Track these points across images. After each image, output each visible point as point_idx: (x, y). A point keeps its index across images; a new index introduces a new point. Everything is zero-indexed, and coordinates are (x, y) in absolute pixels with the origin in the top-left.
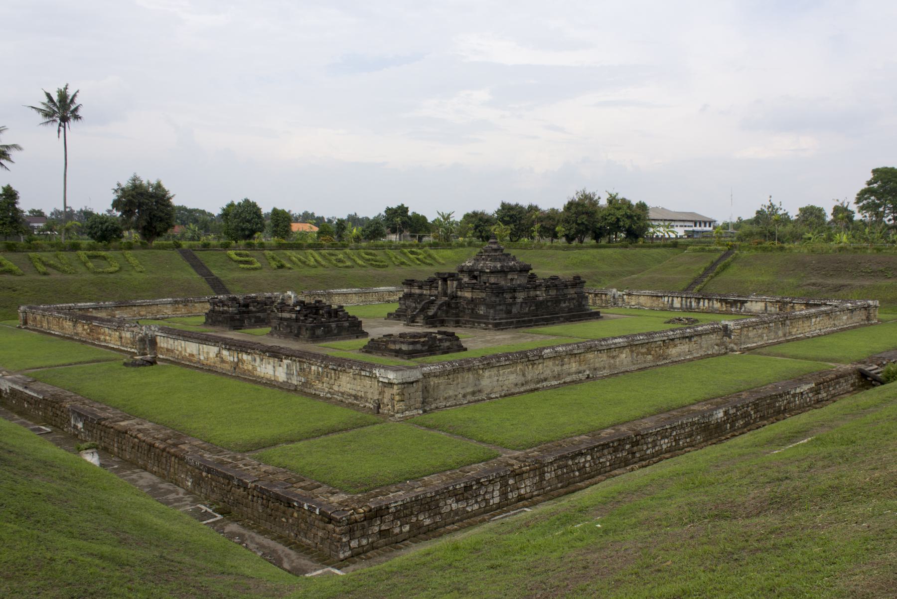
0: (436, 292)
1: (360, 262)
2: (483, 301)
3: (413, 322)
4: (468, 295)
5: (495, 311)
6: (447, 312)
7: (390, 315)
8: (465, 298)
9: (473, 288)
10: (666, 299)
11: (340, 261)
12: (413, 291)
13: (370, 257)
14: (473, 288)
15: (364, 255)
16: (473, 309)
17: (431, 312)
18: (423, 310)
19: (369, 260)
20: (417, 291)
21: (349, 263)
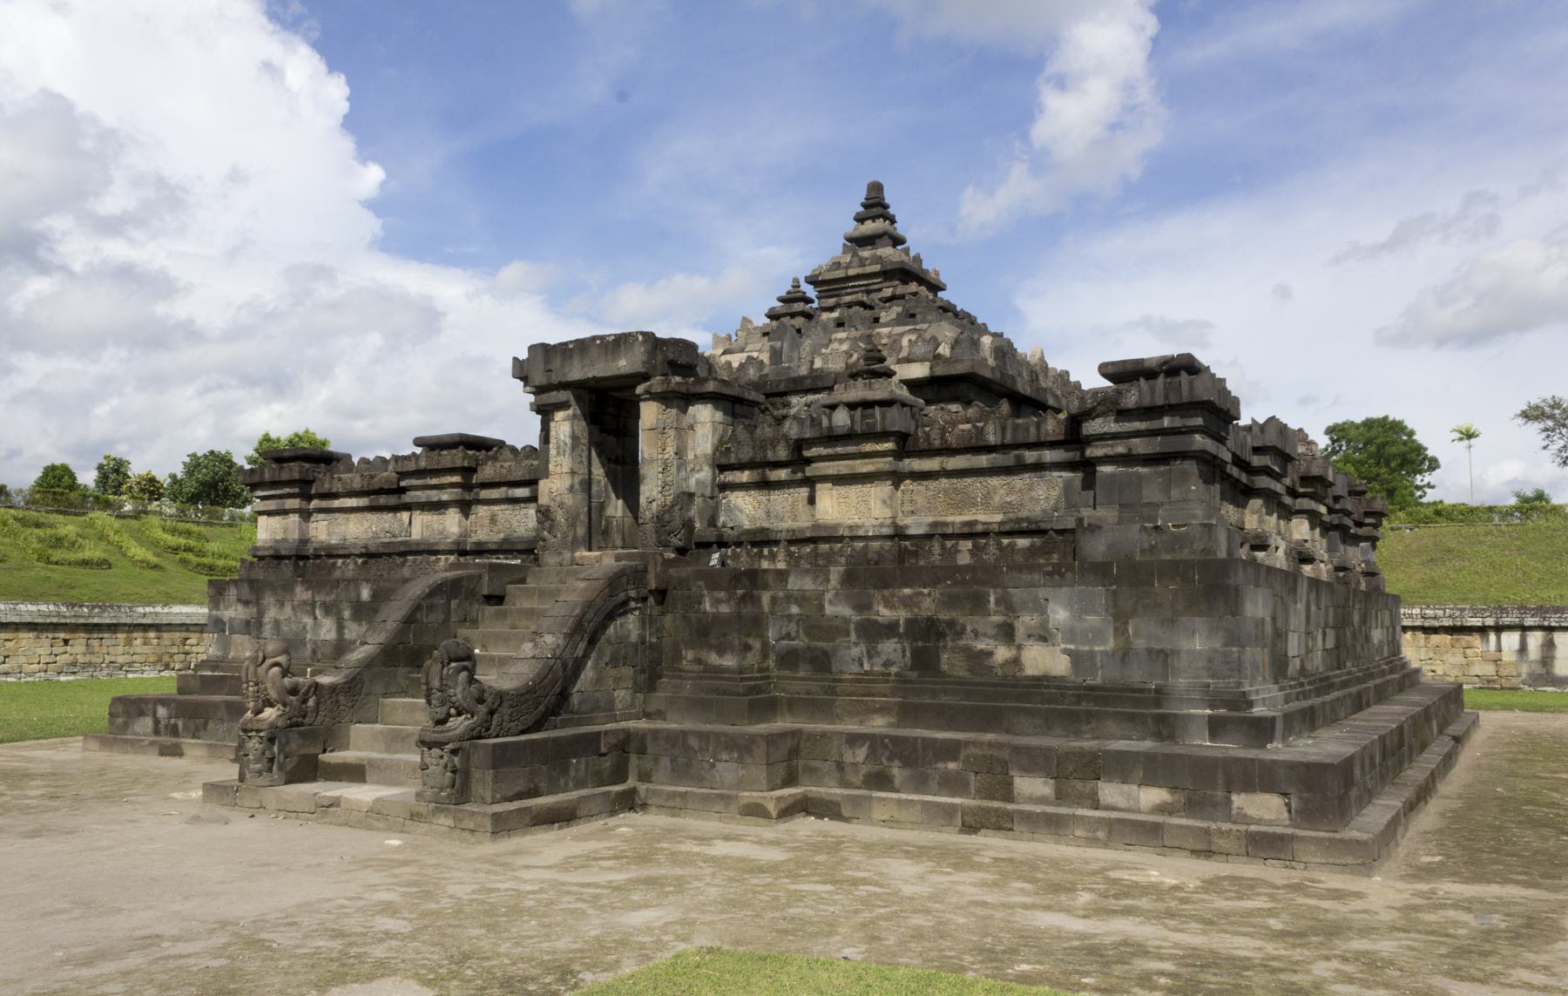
0: (522, 522)
1: (138, 552)
2: (1053, 548)
3: (308, 770)
4: (852, 507)
5: (1233, 639)
6: (651, 670)
7: (129, 708)
8: (816, 543)
9: (906, 445)
10: (1511, 640)
11: (58, 542)
12: (322, 531)
13: (182, 541)
14: (906, 445)
15: (159, 533)
16: (927, 636)
17: (511, 656)
18: (404, 657)
19: (176, 549)
20: (353, 528)
21: (92, 552)
